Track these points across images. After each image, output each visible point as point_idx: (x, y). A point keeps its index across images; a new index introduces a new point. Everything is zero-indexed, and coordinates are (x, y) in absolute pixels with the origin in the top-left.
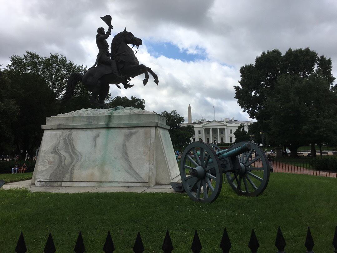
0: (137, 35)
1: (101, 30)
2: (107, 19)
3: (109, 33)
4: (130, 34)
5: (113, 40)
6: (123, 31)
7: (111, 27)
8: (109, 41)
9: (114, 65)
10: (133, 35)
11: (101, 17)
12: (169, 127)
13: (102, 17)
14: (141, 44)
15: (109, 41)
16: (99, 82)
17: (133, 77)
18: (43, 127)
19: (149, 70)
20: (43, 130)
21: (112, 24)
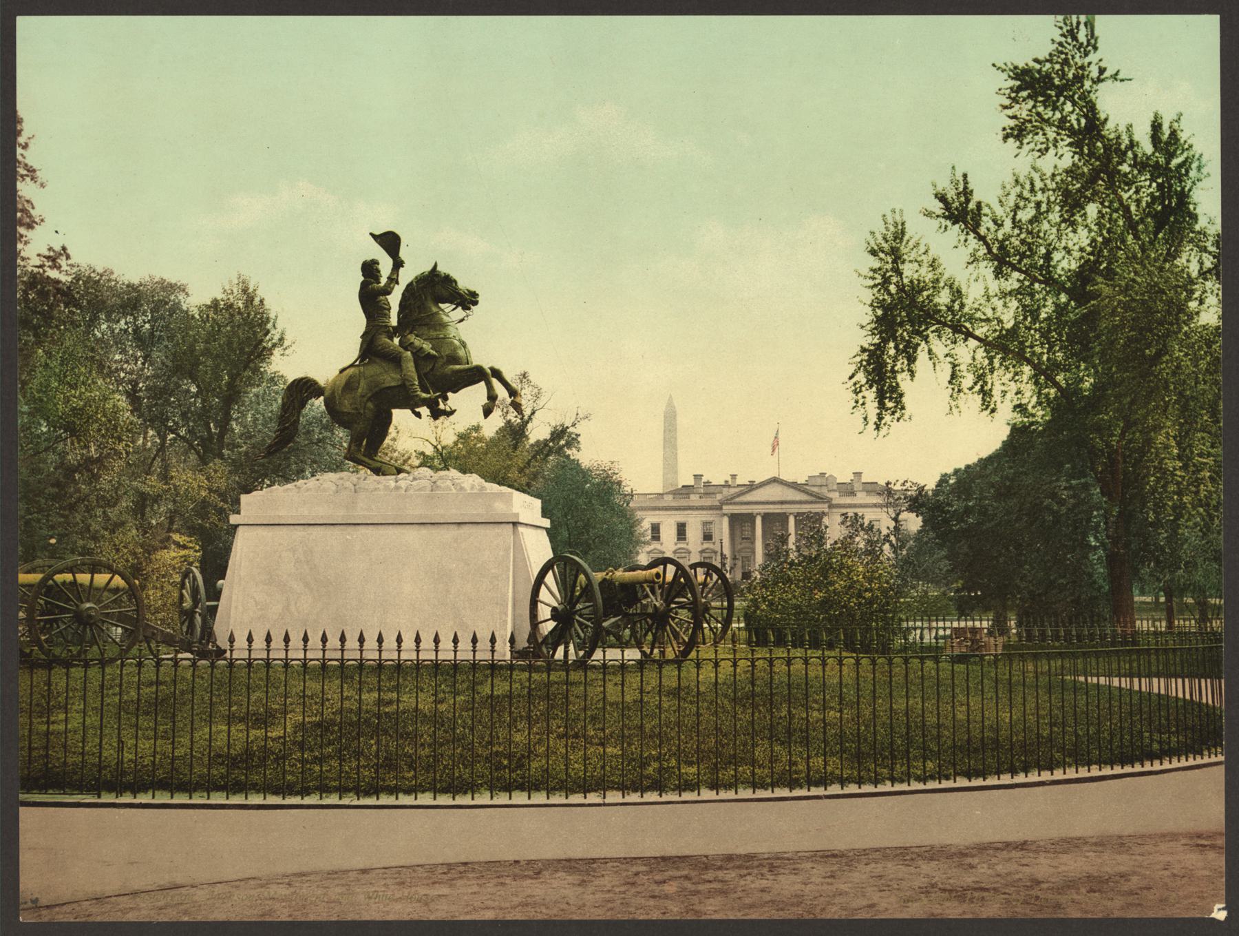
0: (464, 284)
1: (370, 269)
2: (390, 242)
3: (393, 280)
4: (448, 280)
5: (403, 294)
6: (428, 268)
7: (398, 264)
8: (394, 299)
9: (410, 367)
10: (455, 282)
11: (371, 234)
12: (547, 523)
13: (377, 233)
14: (476, 303)
15: (394, 299)
16: (370, 405)
17: (455, 392)
18: (234, 519)
19: (497, 374)
20: (236, 526)
21: (403, 254)
